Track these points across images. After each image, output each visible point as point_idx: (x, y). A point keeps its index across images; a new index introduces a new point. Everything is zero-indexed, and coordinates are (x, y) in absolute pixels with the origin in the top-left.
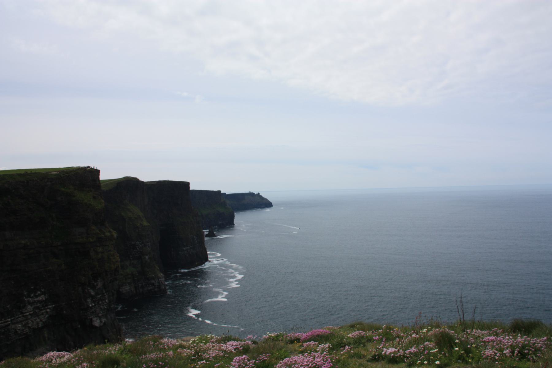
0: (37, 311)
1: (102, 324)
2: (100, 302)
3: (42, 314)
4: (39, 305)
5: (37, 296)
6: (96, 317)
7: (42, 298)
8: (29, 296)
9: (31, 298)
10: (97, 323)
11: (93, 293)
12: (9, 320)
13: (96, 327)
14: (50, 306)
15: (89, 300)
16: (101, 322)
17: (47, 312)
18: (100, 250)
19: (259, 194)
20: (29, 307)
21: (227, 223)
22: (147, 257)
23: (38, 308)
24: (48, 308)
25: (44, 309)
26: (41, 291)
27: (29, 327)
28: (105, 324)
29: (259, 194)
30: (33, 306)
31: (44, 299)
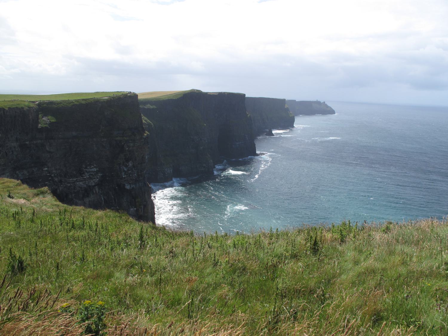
0: (91, 176)
1: (131, 188)
2: (131, 175)
3: (95, 178)
4: (92, 173)
5: (91, 169)
6: (127, 183)
7: (95, 170)
8: (86, 168)
9: (87, 169)
10: (128, 187)
11: (125, 169)
12: (75, 179)
13: (127, 190)
14: (100, 175)
15: (123, 173)
16: (130, 186)
17: (97, 177)
18: (132, 145)
19: (324, 102)
20: (86, 174)
21: (288, 124)
22: (201, 148)
23: (92, 175)
24: (98, 176)
25: (96, 176)
26: (94, 166)
27: (86, 185)
28: (133, 188)
29: (324, 102)
30: (89, 174)
31: (95, 170)
